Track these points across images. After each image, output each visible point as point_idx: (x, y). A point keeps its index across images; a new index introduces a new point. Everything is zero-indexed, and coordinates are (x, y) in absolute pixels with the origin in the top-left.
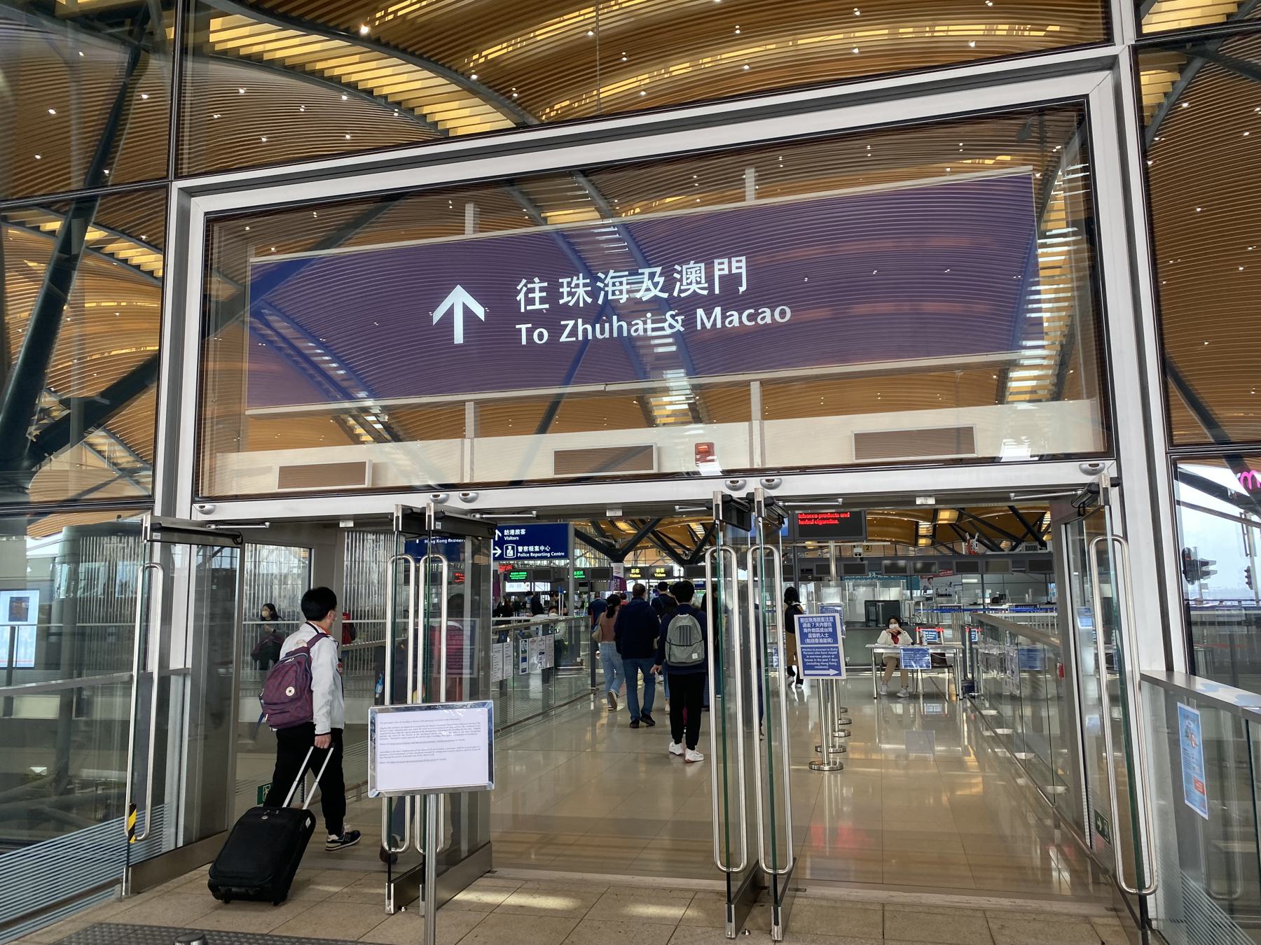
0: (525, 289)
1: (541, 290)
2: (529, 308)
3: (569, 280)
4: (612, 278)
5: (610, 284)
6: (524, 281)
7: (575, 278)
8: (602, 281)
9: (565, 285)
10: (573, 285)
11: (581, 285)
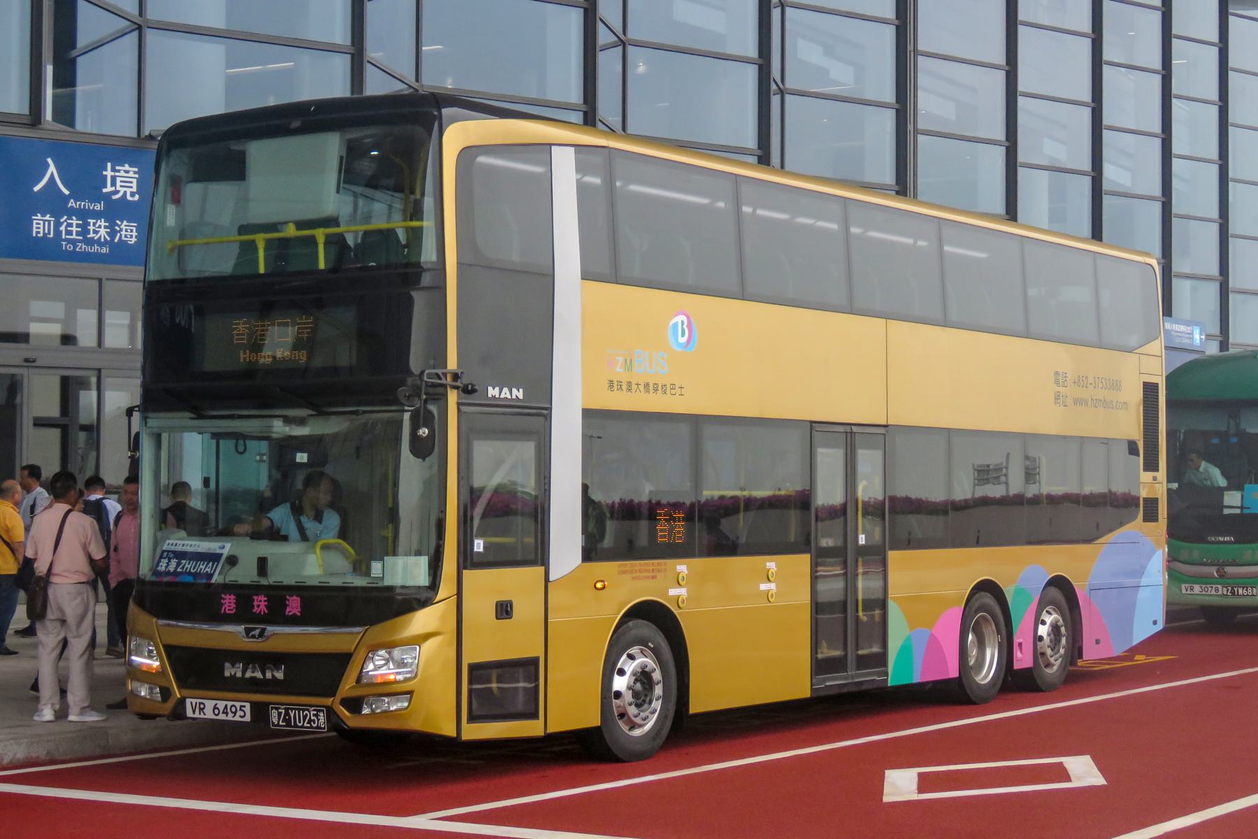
0: (65, 223)
1: (78, 226)
2: (68, 237)
3: (95, 221)
4: (126, 226)
5: (124, 230)
6: (65, 217)
7: (99, 221)
8: (119, 226)
9: (92, 224)
10: (97, 226)
11: (103, 227)
